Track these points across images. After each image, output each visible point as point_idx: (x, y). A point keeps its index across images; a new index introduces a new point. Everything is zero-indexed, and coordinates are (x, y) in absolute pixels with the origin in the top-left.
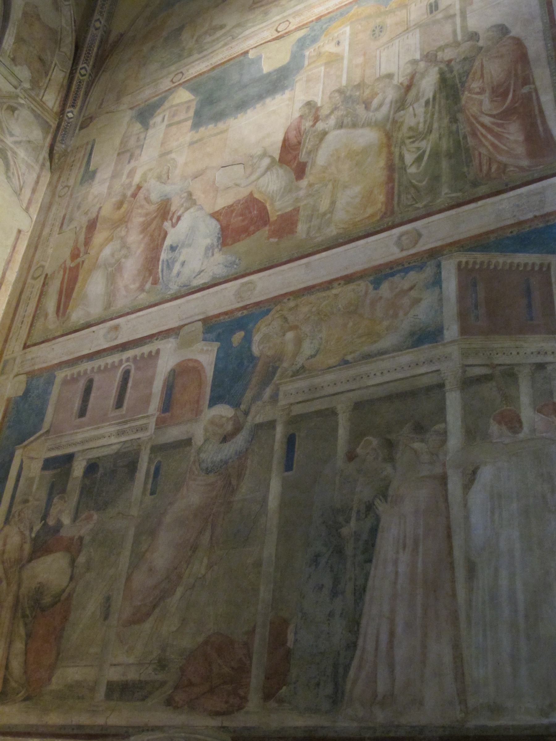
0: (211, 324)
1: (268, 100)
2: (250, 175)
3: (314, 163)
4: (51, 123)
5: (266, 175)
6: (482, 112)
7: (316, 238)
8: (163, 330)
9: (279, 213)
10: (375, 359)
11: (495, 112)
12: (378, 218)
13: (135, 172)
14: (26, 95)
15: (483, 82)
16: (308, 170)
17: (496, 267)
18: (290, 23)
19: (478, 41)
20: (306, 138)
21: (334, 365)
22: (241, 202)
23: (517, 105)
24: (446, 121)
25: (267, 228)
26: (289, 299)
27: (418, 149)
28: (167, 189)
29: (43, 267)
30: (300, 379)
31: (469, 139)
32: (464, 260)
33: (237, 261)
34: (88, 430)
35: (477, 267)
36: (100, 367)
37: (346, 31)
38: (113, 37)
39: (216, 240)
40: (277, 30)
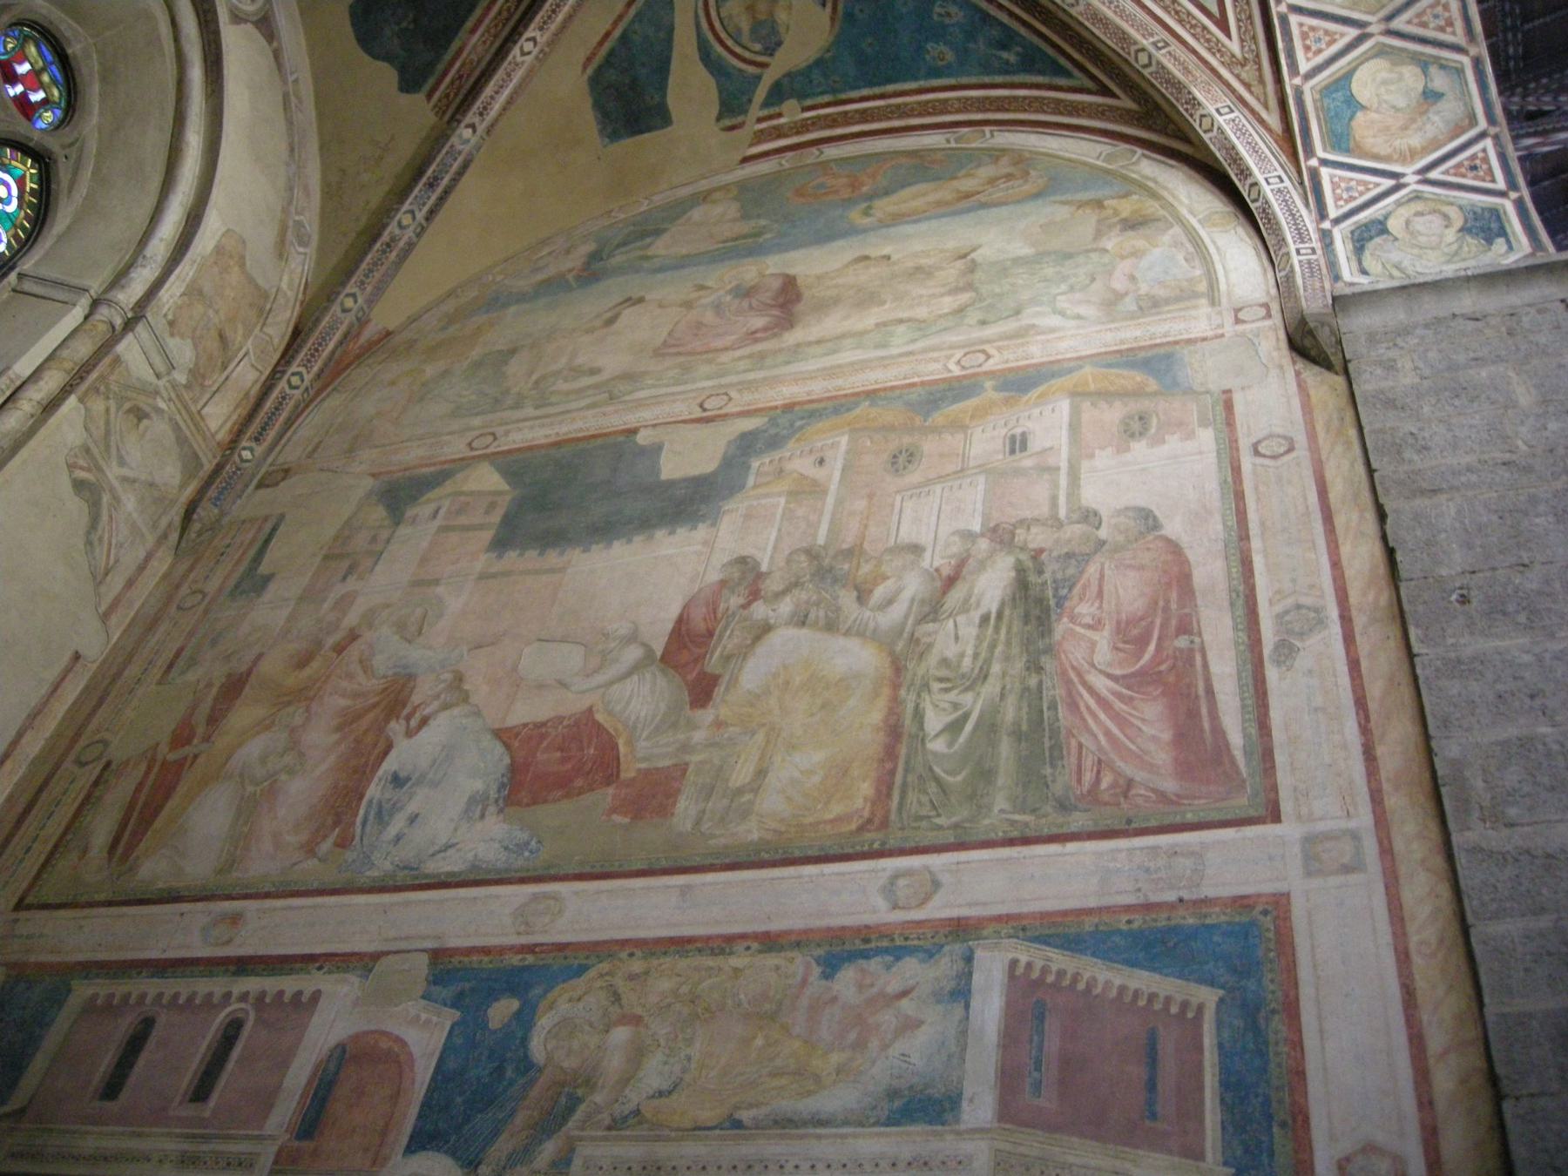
0: (450, 967)
1: (660, 534)
2: (596, 671)
3: (734, 680)
4: (204, 460)
5: (628, 680)
6: (1093, 665)
7: (713, 836)
8: (339, 951)
9: (643, 766)
10: (802, 1131)
11: (1118, 672)
12: (854, 826)
13: (352, 603)
14: (173, 395)
15: (1100, 607)
16: (719, 691)
17: (1090, 986)
18: (730, 399)
19: (1098, 528)
20: (725, 629)
21: (709, 1124)
23: (1163, 667)
24: (1019, 665)
25: (611, 790)
26: (631, 955)
27: (956, 706)
28: (416, 655)
29: (105, 743)
30: (629, 1138)
31: (1062, 711)
32: (1024, 959)
33: (533, 843)
34: (113, 1134)
35: (1050, 979)
36: (176, 996)
37: (839, 442)
38: (368, 333)
39: (494, 787)
40: (701, 406)
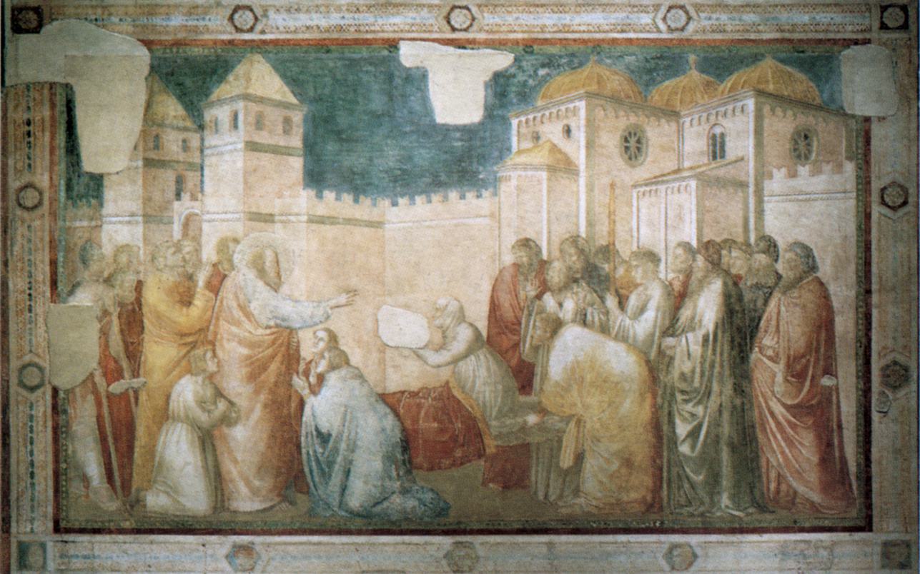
5: (468, 359)
11: (789, 402)
15: (778, 342)
22: (433, 395)
23: (813, 402)
